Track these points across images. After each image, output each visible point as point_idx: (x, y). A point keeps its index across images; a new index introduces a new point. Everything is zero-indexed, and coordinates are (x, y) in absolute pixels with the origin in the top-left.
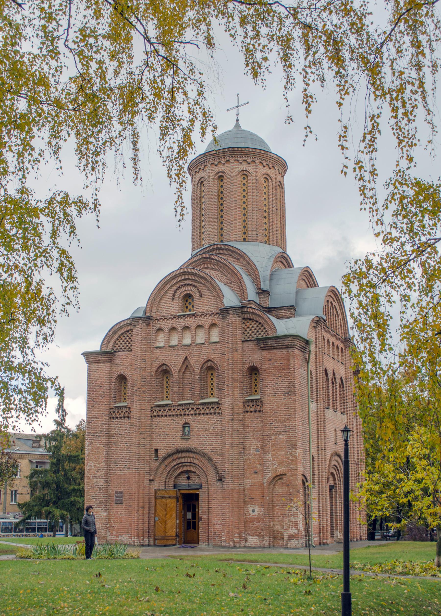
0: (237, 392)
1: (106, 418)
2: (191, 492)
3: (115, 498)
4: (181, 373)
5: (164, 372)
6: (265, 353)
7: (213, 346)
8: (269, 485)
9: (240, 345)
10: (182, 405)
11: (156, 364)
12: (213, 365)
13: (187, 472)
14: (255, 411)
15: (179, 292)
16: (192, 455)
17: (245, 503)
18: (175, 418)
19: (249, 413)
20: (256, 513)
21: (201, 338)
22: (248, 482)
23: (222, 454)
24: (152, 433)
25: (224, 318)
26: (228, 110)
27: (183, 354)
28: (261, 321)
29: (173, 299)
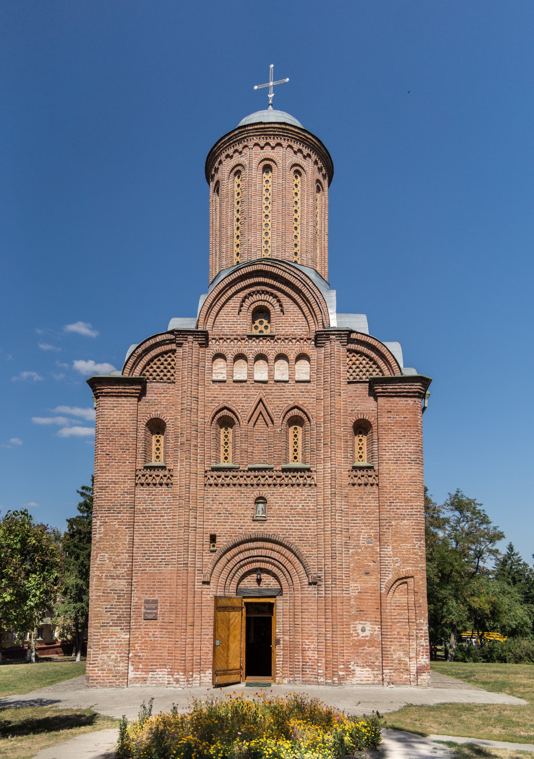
0: (340, 455)
1: (130, 484)
3: (143, 610)
4: (252, 423)
5: (226, 420)
14: (366, 485)
18: (243, 489)
19: (356, 487)
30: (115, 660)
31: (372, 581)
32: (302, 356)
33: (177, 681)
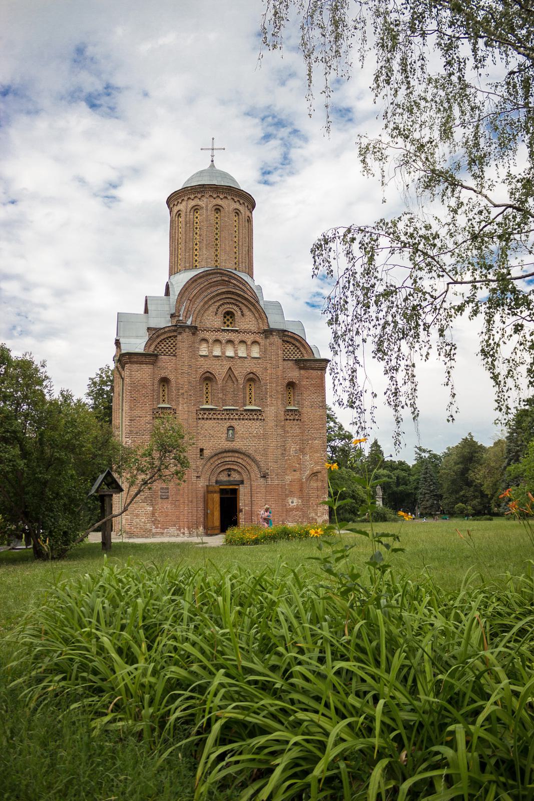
1: (149, 418)
2: (231, 487)
3: (159, 493)
6: (302, 372)
7: (255, 361)
8: (307, 481)
9: (281, 362)
10: (227, 410)
11: (201, 371)
12: (255, 377)
13: (229, 470)
14: (294, 420)
15: (221, 309)
16: (237, 455)
17: (287, 496)
18: (220, 421)
20: (295, 504)
21: (242, 352)
22: (288, 478)
23: (265, 455)
24: (198, 433)
25: (266, 338)
26: (202, 149)
27: (227, 365)
28: (298, 344)
29: (216, 314)
30: (144, 522)
31: (297, 475)
32: (255, 342)
33: (184, 533)
